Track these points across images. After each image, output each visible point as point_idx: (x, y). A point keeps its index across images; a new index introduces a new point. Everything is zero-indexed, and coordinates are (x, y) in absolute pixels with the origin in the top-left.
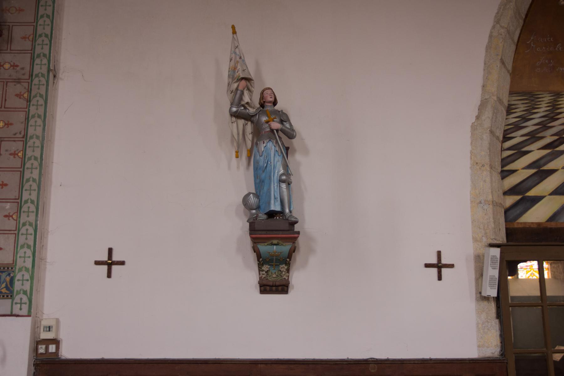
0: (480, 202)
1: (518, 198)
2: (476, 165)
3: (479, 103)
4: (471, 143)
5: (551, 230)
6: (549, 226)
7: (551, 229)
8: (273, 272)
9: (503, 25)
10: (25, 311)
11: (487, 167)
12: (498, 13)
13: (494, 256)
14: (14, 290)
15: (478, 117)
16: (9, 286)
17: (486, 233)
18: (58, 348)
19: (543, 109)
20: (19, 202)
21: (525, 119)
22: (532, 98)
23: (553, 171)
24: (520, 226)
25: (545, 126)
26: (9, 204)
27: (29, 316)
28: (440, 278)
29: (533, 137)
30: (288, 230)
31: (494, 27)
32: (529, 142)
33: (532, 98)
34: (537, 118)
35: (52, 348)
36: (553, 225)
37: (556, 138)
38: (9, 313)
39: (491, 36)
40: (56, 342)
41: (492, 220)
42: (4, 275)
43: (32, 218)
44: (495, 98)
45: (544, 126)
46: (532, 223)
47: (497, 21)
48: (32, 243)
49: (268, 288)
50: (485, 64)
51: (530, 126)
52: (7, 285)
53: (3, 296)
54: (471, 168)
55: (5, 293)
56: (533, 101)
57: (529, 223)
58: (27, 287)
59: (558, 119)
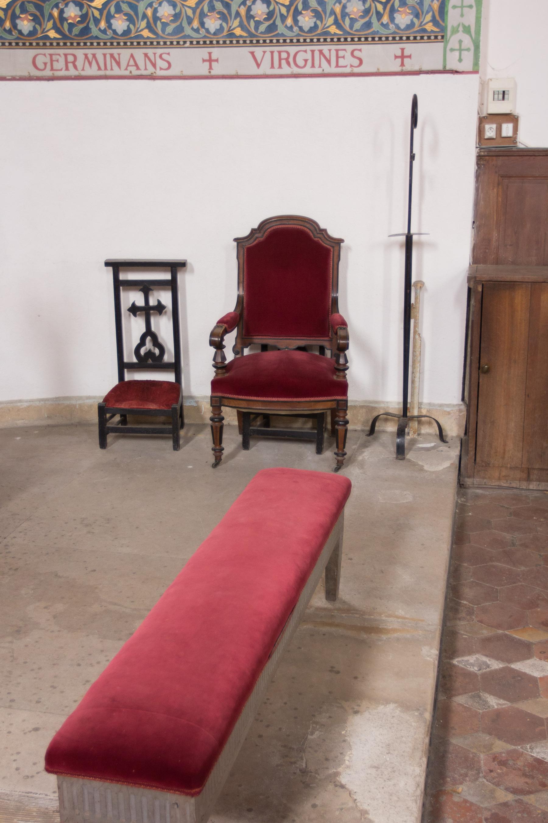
10: (467, 65)
14: (447, 26)
16: (438, 18)
18: (516, 130)
27: (476, 72)
35: (507, 130)
38: (441, 68)
52: (434, 17)
53: (429, 38)
55: (432, 31)
58: (470, 19)
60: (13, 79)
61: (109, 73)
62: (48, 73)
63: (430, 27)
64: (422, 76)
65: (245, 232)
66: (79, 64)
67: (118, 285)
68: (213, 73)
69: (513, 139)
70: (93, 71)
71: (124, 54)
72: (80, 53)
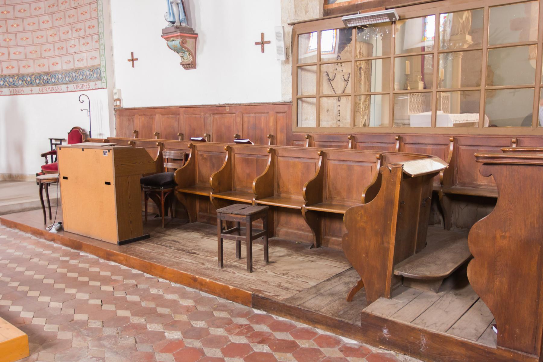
8: (186, 56)
13: (278, 32)
17: (289, 16)
18: (120, 103)
20: (98, 34)
26: (96, 36)
27: (106, 88)
28: (263, 51)
30: (175, 32)
38: (101, 87)
40: (118, 100)
41: (293, 6)
42: (98, 70)
43: (103, 42)
46: (345, 2)
48: (104, 54)
49: (186, 66)
57: (342, 2)
60: (35, 94)
61: (52, 92)
62: (42, 92)
63: (99, 77)
64: (99, 90)
65: (69, 132)
66: (47, 90)
67: (52, 144)
68: (68, 91)
69: (120, 105)
70: (49, 91)
71: (54, 87)
72: (47, 87)
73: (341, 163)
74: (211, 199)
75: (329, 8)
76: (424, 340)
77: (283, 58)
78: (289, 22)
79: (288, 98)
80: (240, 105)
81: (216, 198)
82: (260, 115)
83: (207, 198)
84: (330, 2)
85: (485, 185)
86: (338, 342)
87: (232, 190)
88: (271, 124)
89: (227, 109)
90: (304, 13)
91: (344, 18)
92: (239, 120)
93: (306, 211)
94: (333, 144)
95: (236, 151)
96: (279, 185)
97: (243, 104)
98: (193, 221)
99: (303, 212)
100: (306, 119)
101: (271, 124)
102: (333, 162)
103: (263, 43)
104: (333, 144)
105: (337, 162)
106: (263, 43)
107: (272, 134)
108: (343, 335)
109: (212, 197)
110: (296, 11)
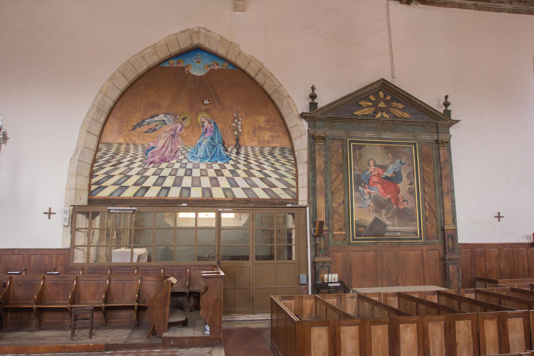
0: (70, 189)
1: (98, 186)
2: (70, 174)
3: (75, 149)
4: (69, 165)
5: (109, 200)
6: (109, 198)
7: (109, 199)
9: (90, 117)
11: (75, 175)
12: (88, 112)
15: (74, 155)
17: (71, 201)
19: (113, 150)
21: (105, 154)
22: (109, 145)
23: (113, 176)
24: (97, 198)
25: (113, 157)
29: (108, 162)
31: (86, 117)
32: (106, 164)
33: (109, 145)
34: (110, 154)
36: (110, 197)
37: (117, 162)
39: (84, 121)
41: (74, 196)
44: (82, 147)
45: (113, 157)
47: (88, 115)
50: (80, 133)
51: (107, 157)
54: (68, 175)
56: (109, 146)
59: (119, 154)
73: (119, 282)
74: (34, 309)
75: (92, 198)
76: (187, 340)
77: (67, 224)
78: (70, 204)
79: (68, 245)
80: (28, 250)
81: (38, 308)
82: (45, 256)
83: (32, 308)
84: (92, 195)
85: (177, 287)
86: (154, 352)
87: (43, 302)
88: (54, 261)
89: (16, 252)
90: (79, 200)
91: (109, 208)
92: (26, 259)
93: (105, 307)
94: (97, 272)
95: (48, 279)
96: (79, 297)
97: (32, 249)
98: (5, 328)
99: (103, 308)
100: (77, 258)
101: (54, 261)
102: (114, 282)
103: (49, 213)
104: (97, 272)
105: (116, 282)
106: (49, 213)
107: (54, 267)
108: (154, 349)
109: (36, 307)
110: (75, 199)
